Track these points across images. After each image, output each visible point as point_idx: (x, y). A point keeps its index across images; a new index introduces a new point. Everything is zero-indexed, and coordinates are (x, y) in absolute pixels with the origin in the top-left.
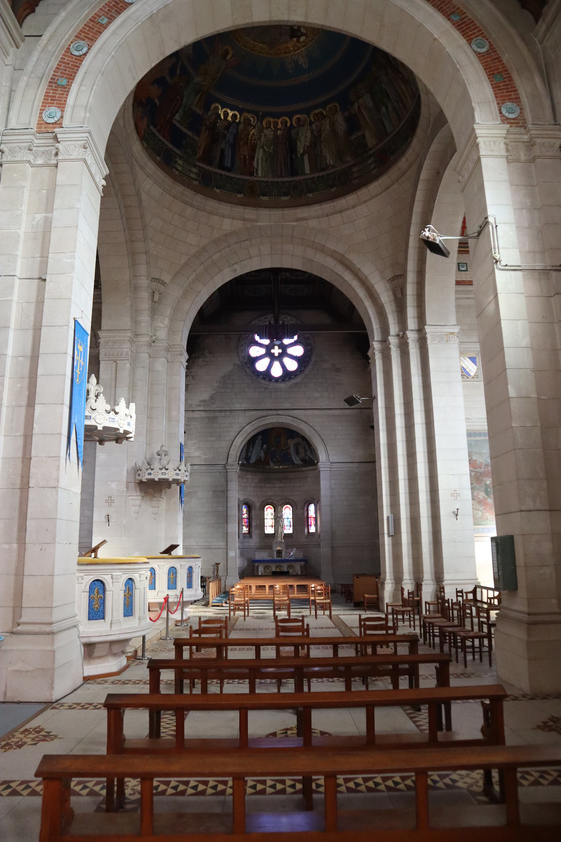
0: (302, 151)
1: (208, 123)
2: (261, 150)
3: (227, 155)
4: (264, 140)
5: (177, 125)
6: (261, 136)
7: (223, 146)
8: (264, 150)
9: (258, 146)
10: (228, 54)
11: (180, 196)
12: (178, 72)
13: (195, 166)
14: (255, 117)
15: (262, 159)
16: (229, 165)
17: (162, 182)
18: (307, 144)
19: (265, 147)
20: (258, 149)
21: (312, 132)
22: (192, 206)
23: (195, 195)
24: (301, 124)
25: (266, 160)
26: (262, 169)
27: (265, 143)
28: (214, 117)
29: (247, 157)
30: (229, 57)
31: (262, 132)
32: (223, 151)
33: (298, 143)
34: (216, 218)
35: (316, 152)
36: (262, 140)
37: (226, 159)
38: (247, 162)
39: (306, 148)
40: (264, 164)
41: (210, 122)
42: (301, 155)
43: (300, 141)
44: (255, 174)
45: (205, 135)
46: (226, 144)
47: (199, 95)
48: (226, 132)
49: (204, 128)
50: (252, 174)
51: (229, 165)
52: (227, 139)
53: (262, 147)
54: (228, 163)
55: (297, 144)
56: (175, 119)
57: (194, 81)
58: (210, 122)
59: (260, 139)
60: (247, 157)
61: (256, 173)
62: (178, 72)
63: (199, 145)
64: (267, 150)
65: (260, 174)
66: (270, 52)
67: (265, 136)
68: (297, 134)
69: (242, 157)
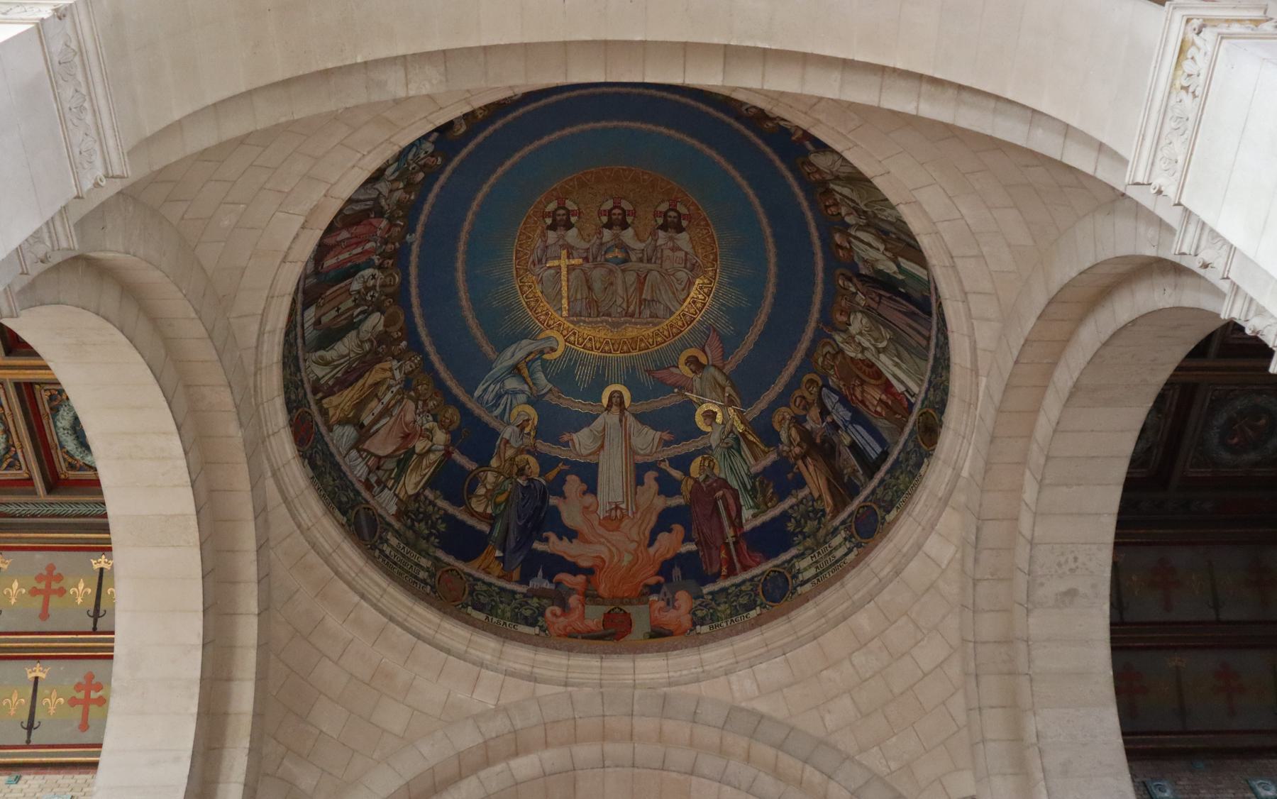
0: (894, 268)
1: (797, 450)
2: (882, 357)
3: (863, 442)
4: (869, 341)
5: (758, 522)
6: (860, 343)
7: (847, 441)
8: (884, 350)
9: (874, 360)
10: (696, 359)
11: (823, 620)
12: (677, 474)
13: (835, 532)
14: (826, 340)
15: (896, 365)
16: (879, 450)
17: (767, 645)
18: (882, 247)
19: (880, 346)
20: (879, 365)
21: (860, 228)
22: (857, 608)
23: (843, 586)
24: (848, 246)
25: (899, 357)
26: (909, 377)
27: (873, 342)
28: (793, 432)
29: (884, 397)
30: (703, 360)
31: (853, 337)
32: (853, 446)
33: (881, 267)
34: (913, 565)
35: (894, 236)
36: (866, 344)
37: (868, 448)
38: (890, 403)
39: (887, 254)
40: (904, 366)
41: (798, 445)
42: (900, 273)
43: (877, 260)
44: (913, 400)
45: (811, 468)
46: (846, 432)
47: (743, 443)
48: (829, 419)
49: (800, 463)
50: (911, 405)
51: (879, 450)
52: (840, 423)
53: (879, 351)
54: (874, 450)
55: (882, 270)
56: (747, 520)
57: (714, 446)
58: (798, 445)
59: (864, 349)
60: (884, 397)
61: (912, 396)
62: (677, 474)
63: (816, 495)
64: (884, 344)
65: (915, 389)
66: (710, 273)
67: (860, 333)
68: (865, 261)
69: (879, 409)
